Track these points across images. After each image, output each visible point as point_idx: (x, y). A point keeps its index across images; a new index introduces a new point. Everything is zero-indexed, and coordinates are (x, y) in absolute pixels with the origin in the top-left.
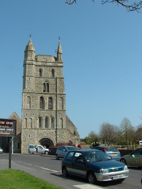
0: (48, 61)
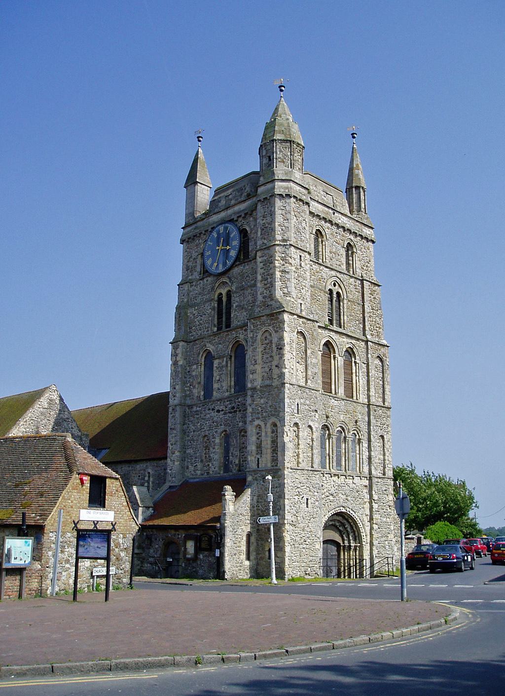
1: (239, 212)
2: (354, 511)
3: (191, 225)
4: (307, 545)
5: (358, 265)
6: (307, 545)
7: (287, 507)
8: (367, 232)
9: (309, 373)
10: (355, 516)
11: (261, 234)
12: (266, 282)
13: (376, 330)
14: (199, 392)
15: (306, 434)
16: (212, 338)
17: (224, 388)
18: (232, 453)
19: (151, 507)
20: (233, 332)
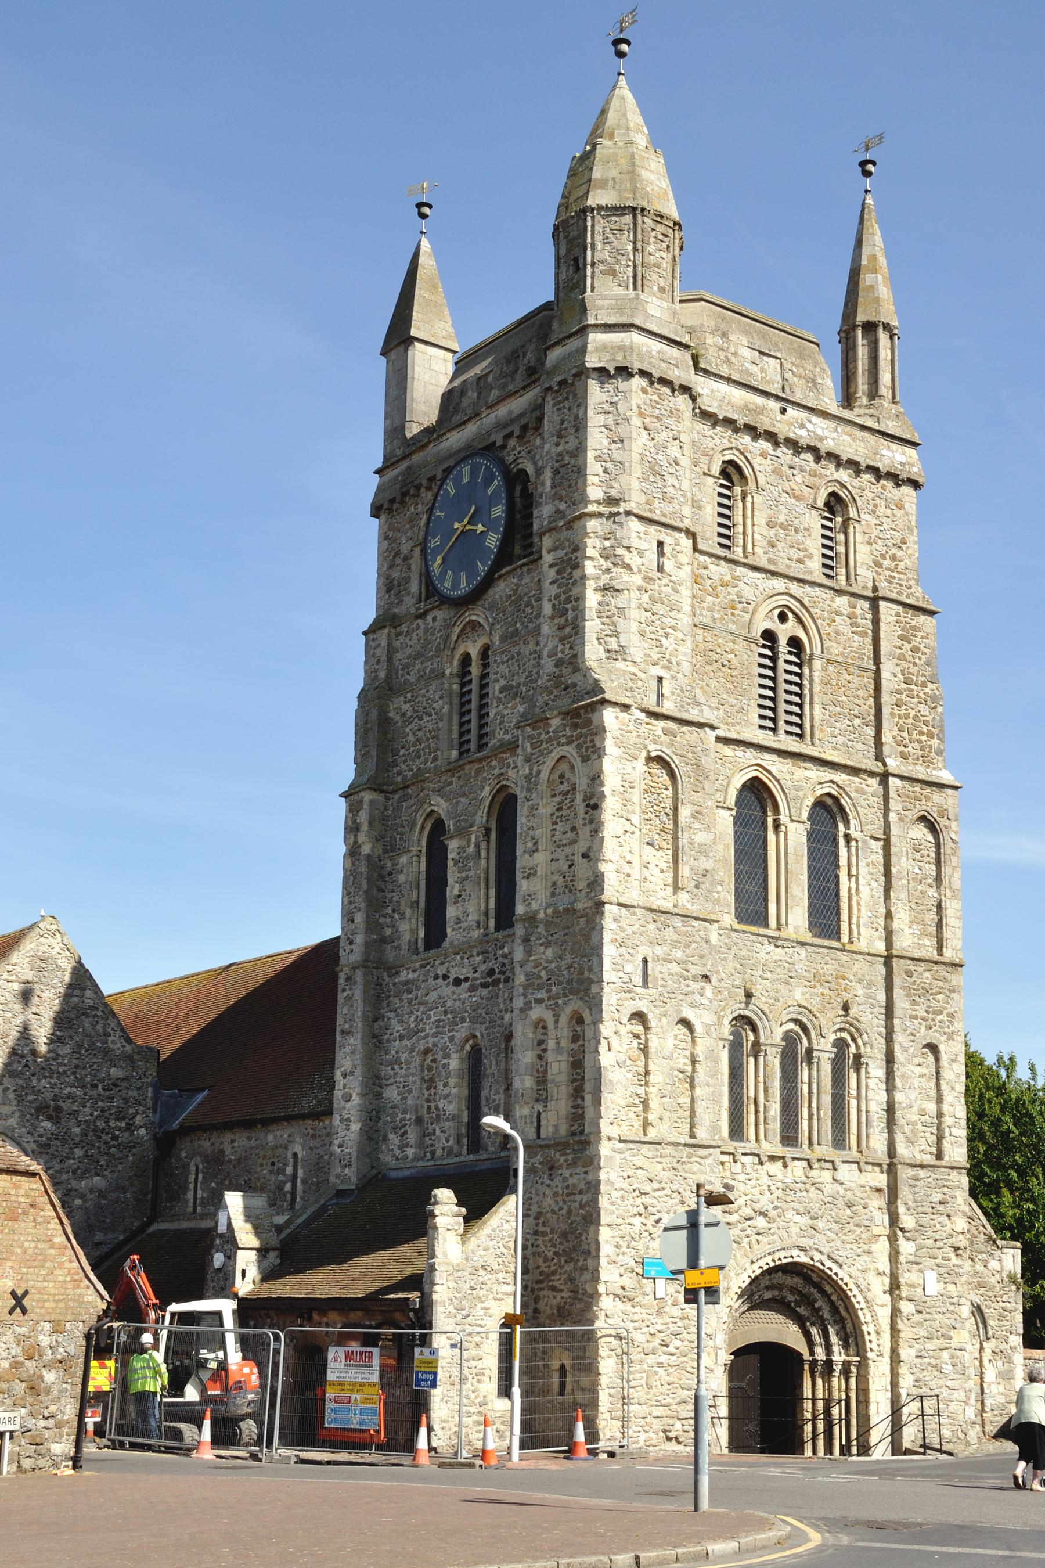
0: (798, 397)
1: (505, 425)
2: (836, 1262)
3: (397, 462)
4: (672, 1355)
5: (862, 554)
6: (672, 1355)
7: (606, 1250)
8: (893, 457)
9: (685, 871)
10: (843, 1275)
11: (553, 486)
12: (562, 620)
13: (919, 741)
14: (414, 931)
15: (670, 1042)
16: (443, 778)
17: (470, 918)
18: (487, 1100)
19: (274, 1249)
20: (494, 763)
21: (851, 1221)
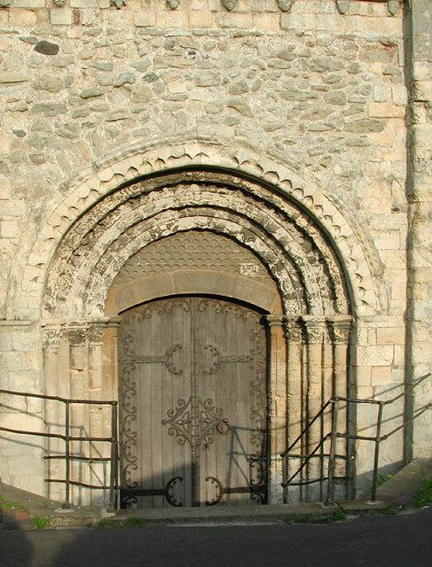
2: (285, 162)
21: (321, 95)
